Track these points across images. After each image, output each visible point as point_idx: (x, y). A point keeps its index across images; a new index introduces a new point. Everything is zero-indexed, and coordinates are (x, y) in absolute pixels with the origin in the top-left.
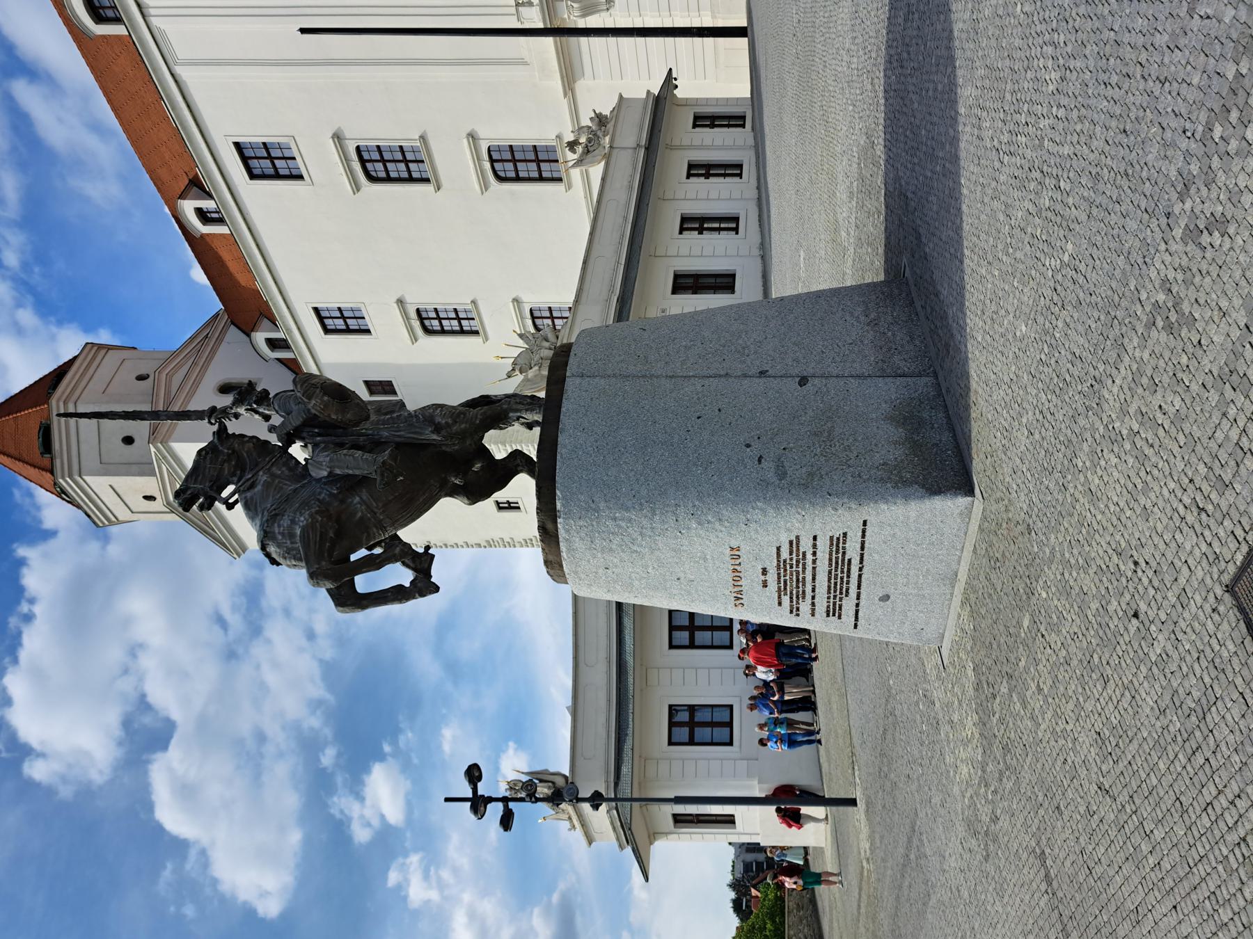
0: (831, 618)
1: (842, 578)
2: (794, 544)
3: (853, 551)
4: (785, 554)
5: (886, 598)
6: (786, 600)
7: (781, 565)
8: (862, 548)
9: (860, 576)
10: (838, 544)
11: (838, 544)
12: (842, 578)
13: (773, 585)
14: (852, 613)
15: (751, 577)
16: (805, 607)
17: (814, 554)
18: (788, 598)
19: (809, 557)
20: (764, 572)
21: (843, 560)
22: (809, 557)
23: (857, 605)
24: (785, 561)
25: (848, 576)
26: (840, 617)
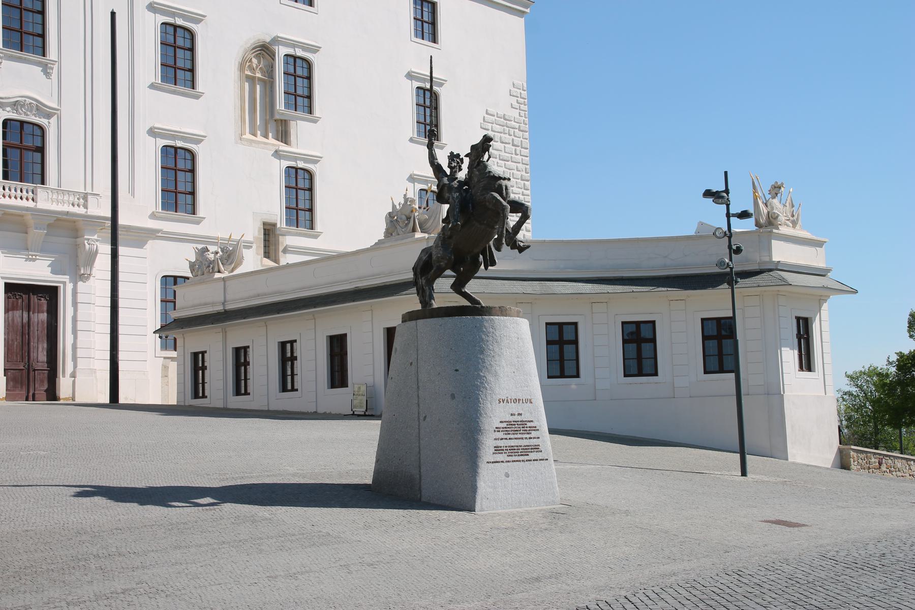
0: (493, 450)
2: (535, 429)
3: (533, 456)
4: (529, 424)
5: (507, 475)
7: (524, 423)
10: (536, 448)
11: (536, 448)
13: (512, 418)
14: (498, 460)
15: (514, 408)
16: (501, 435)
18: (504, 425)
19: (528, 436)
20: (520, 414)
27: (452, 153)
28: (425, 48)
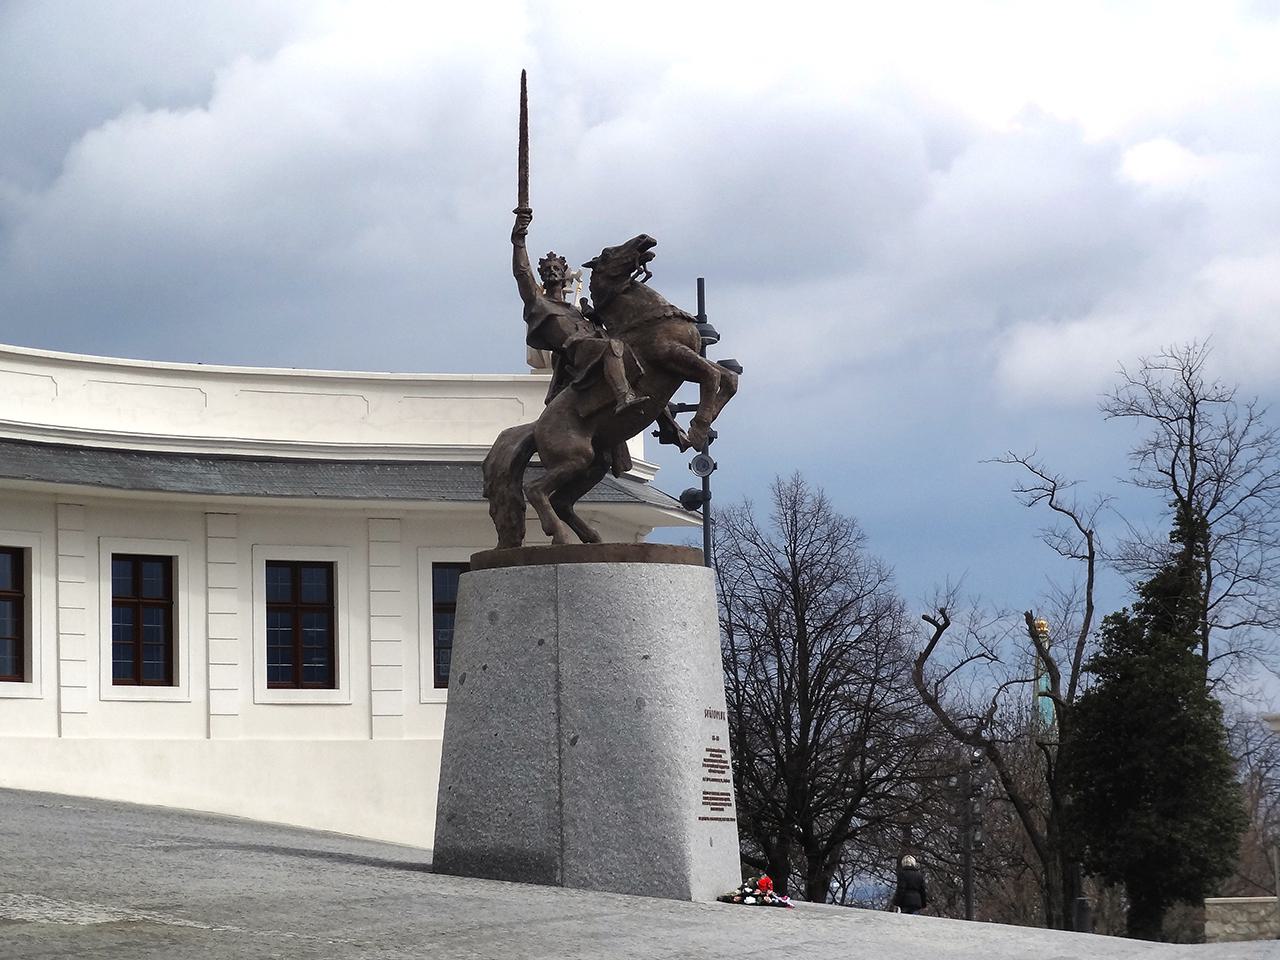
27: (551, 256)
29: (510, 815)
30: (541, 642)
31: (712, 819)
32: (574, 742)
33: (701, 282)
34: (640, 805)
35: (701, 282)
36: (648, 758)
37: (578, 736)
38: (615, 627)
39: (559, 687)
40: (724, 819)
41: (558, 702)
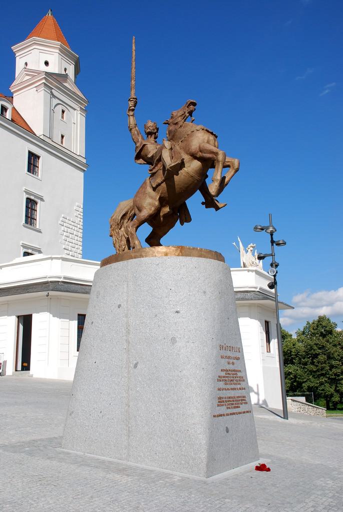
0: (217, 401)
1: (233, 404)
6: (223, 374)
8: (244, 412)
9: (234, 414)
12: (233, 404)
17: (240, 389)
19: (239, 386)
21: (238, 404)
22: (239, 386)
23: (224, 415)
24: (236, 374)
25: (235, 407)
26: (218, 405)
28: (30, 177)
29: (101, 412)
30: (119, 306)
31: (228, 415)
32: (136, 366)
33: (270, 215)
34: (173, 407)
35: (270, 215)
36: (178, 376)
37: (138, 362)
38: (159, 294)
39: (128, 332)
40: (240, 413)
41: (128, 342)
